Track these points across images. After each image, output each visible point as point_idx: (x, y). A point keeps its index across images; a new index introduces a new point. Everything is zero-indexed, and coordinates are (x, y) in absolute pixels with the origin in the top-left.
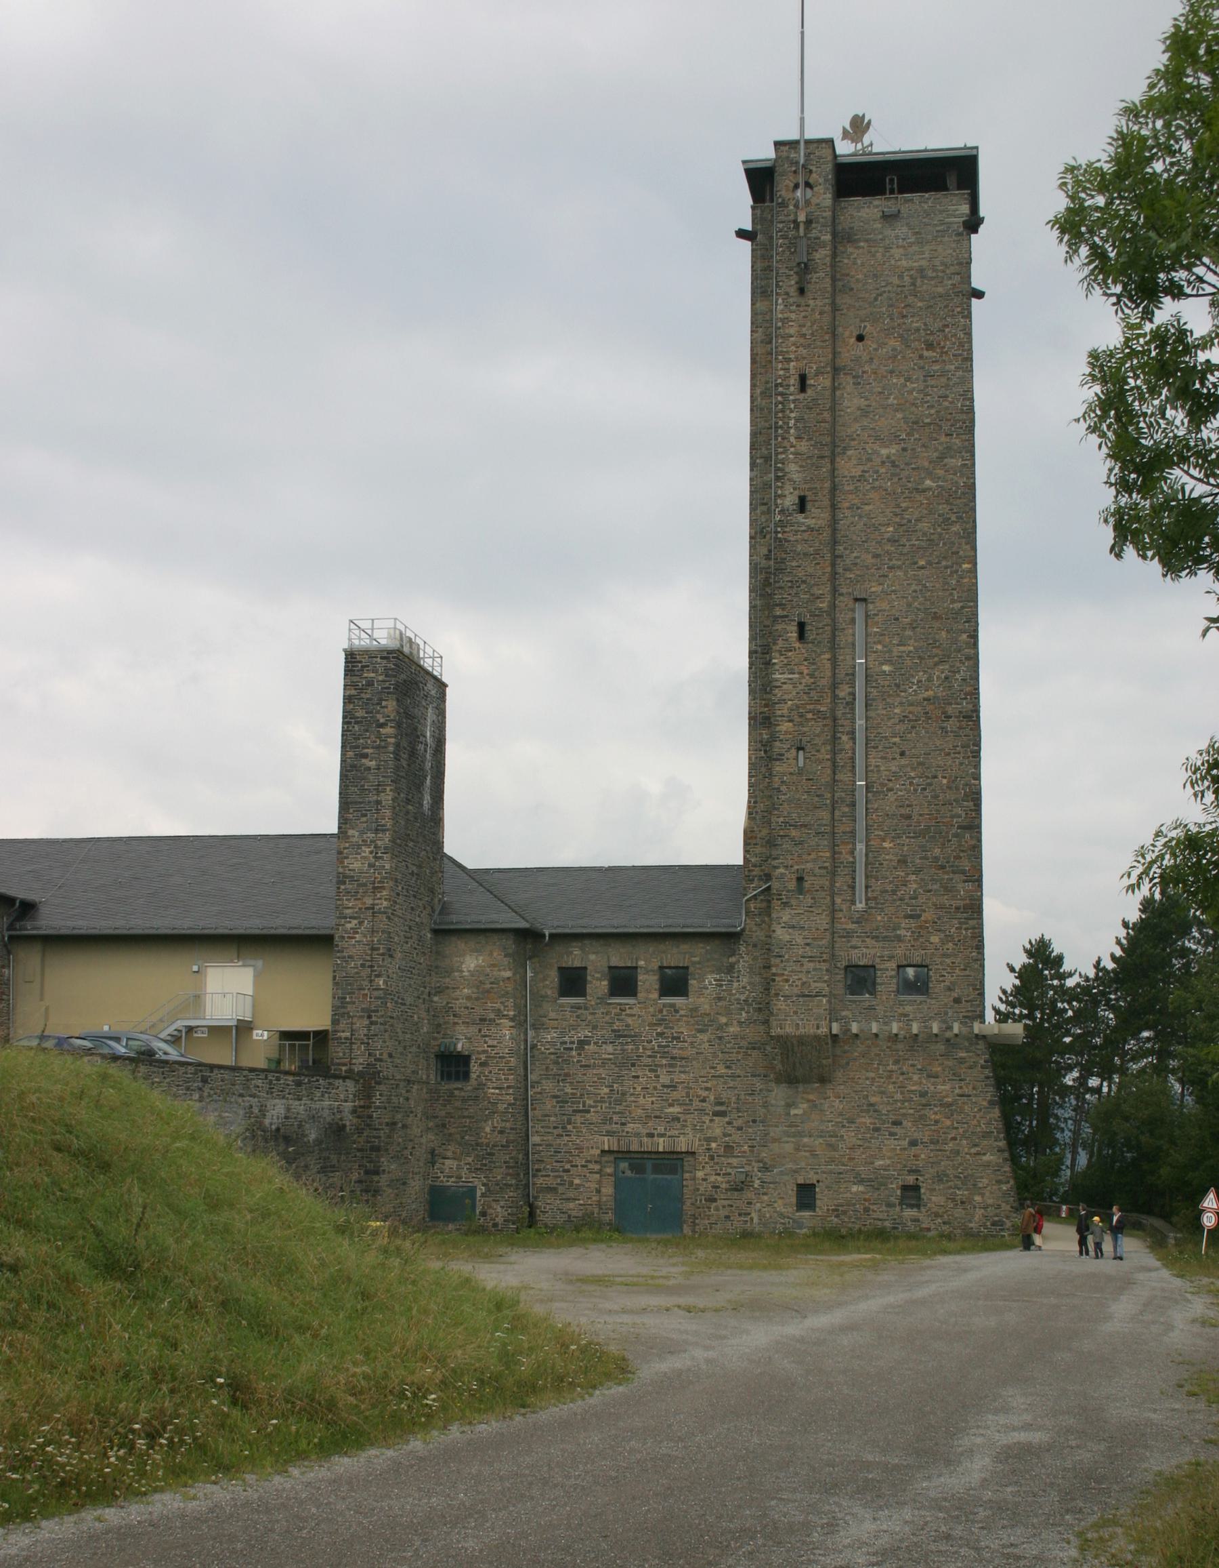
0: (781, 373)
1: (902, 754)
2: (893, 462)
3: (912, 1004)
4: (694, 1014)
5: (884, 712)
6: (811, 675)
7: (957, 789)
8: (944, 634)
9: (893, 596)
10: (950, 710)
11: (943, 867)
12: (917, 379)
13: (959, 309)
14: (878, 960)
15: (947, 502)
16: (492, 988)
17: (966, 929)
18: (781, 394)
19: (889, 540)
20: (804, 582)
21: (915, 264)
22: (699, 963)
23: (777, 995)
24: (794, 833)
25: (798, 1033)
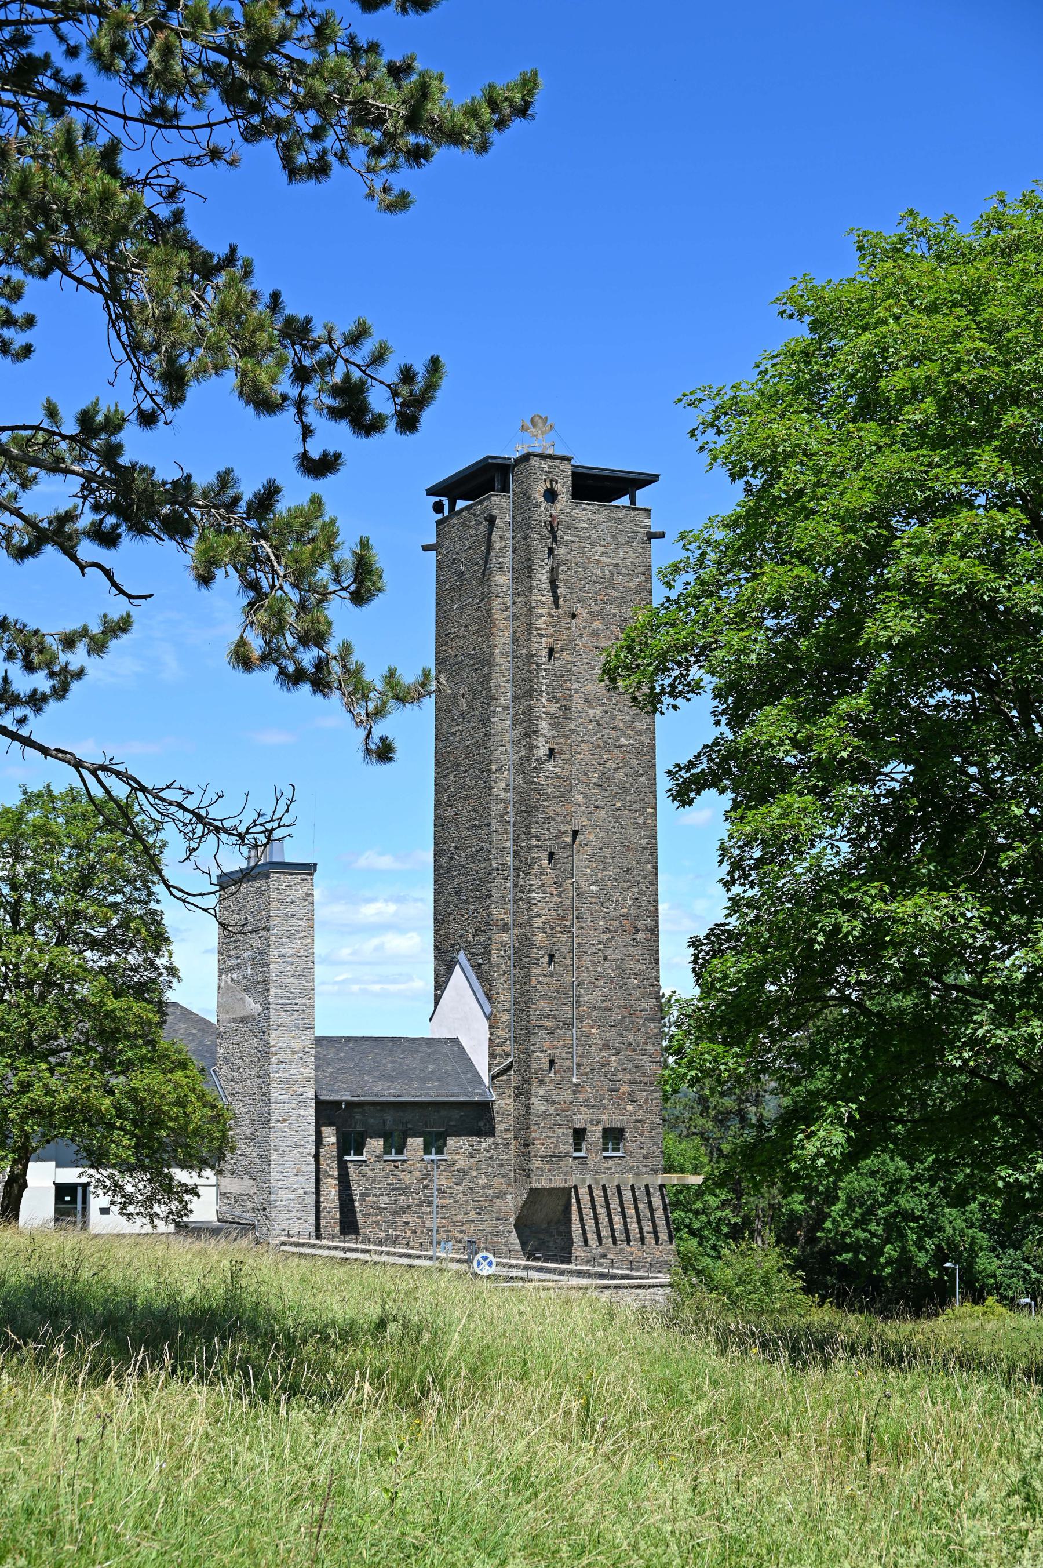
1: (605, 959)
6: (559, 896)
8: (634, 864)
10: (639, 924)
11: (634, 1051)
15: (636, 758)
18: (537, 664)
24: (547, 1024)
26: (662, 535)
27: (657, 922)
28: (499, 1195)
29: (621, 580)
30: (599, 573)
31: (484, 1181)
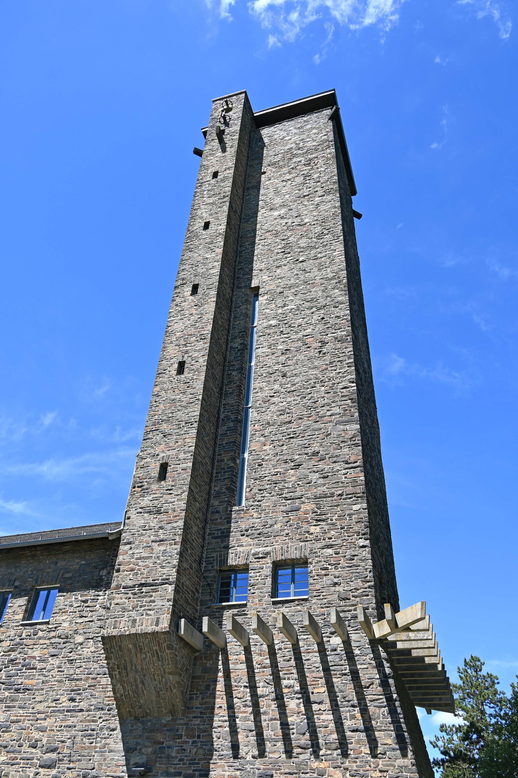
4: (53, 634)
14: (251, 559)
22: (70, 578)
25: (133, 631)
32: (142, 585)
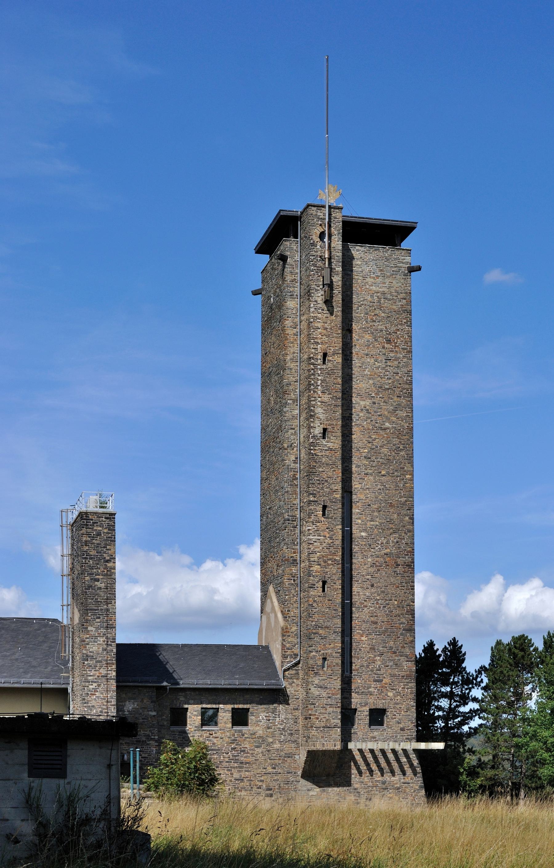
0: (313, 350)
1: (372, 586)
2: (368, 410)
3: (377, 732)
4: (254, 736)
5: (362, 560)
6: (331, 538)
7: (403, 607)
8: (396, 516)
9: (368, 491)
10: (399, 561)
11: (395, 653)
12: (381, 361)
13: (405, 321)
14: (358, 706)
16: (144, 722)
17: (408, 689)
18: (313, 364)
19: (365, 457)
20: (326, 481)
21: (380, 290)
23: (312, 727)
24: (321, 631)
25: (324, 749)
26: (419, 269)
27: (413, 559)
28: (290, 756)
29: (386, 304)
30: (369, 298)
31: (277, 746)
32: (324, 727)
